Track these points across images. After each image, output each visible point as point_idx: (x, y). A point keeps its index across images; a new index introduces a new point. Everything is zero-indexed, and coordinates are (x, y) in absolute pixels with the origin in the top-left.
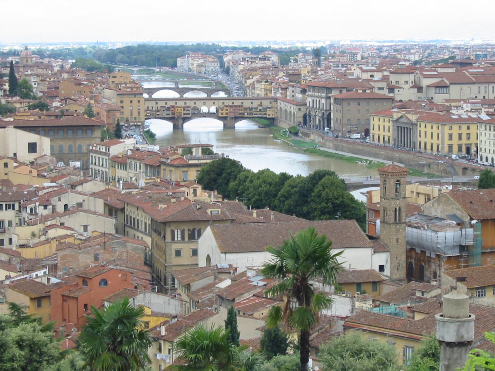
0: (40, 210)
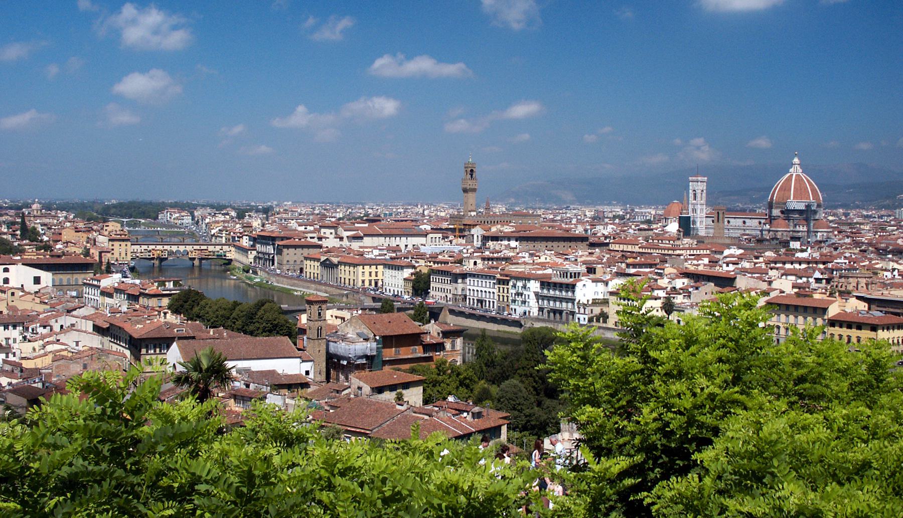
0: (41, 330)
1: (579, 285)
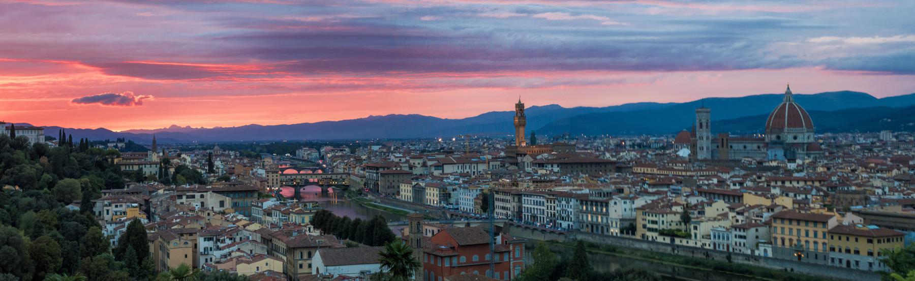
1: (611, 203)
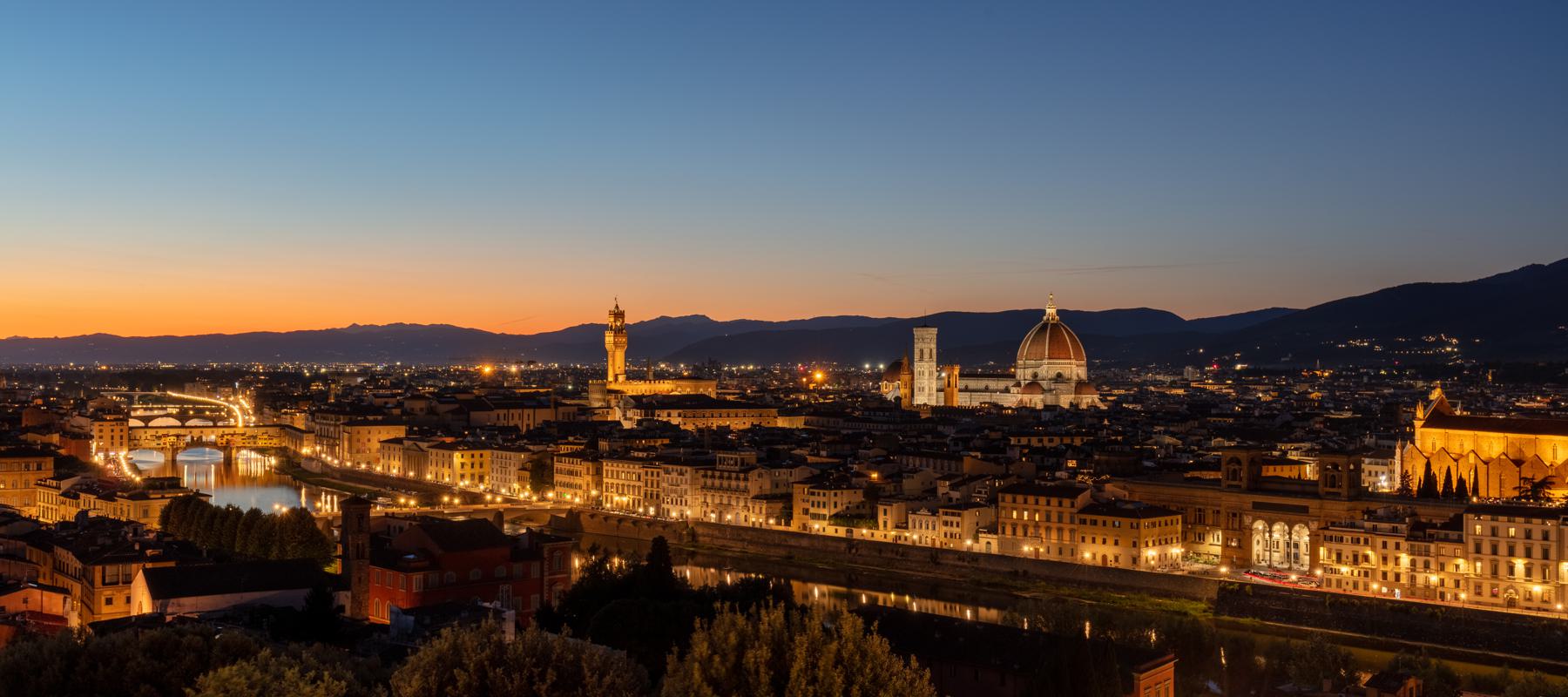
1: (753, 475)
